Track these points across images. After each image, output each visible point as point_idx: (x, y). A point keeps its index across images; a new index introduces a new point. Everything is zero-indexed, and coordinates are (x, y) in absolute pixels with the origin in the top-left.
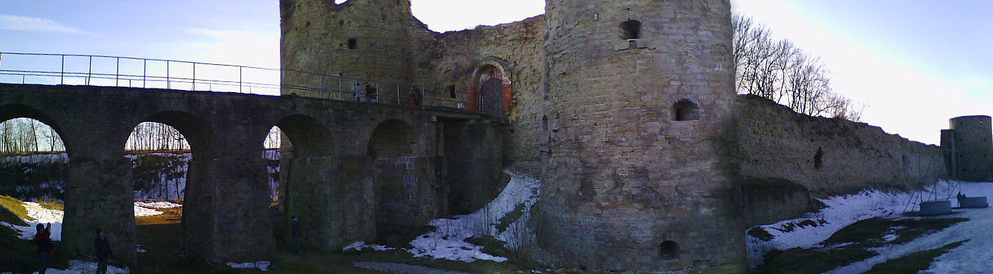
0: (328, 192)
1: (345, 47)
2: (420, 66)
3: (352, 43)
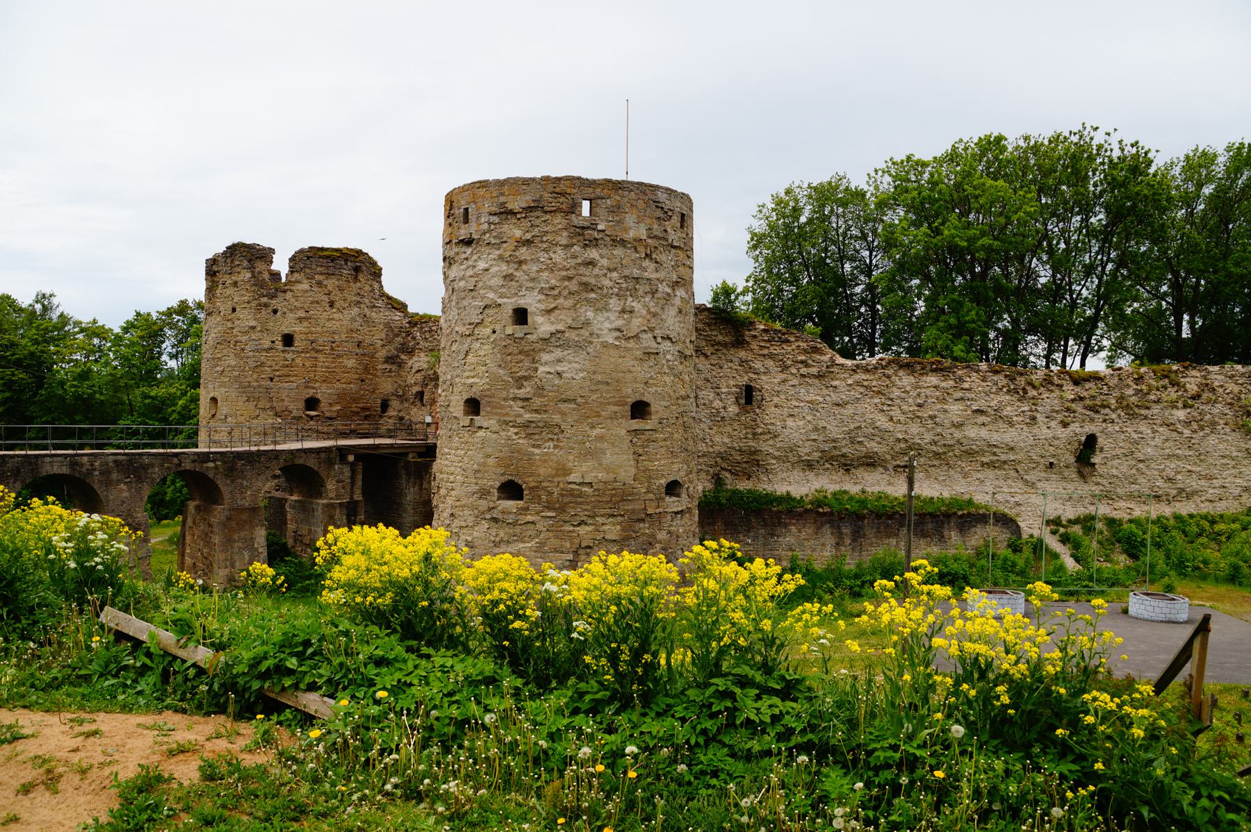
0: (216, 541)
1: (279, 346)
2: (386, 362)
3: (288, 340)
